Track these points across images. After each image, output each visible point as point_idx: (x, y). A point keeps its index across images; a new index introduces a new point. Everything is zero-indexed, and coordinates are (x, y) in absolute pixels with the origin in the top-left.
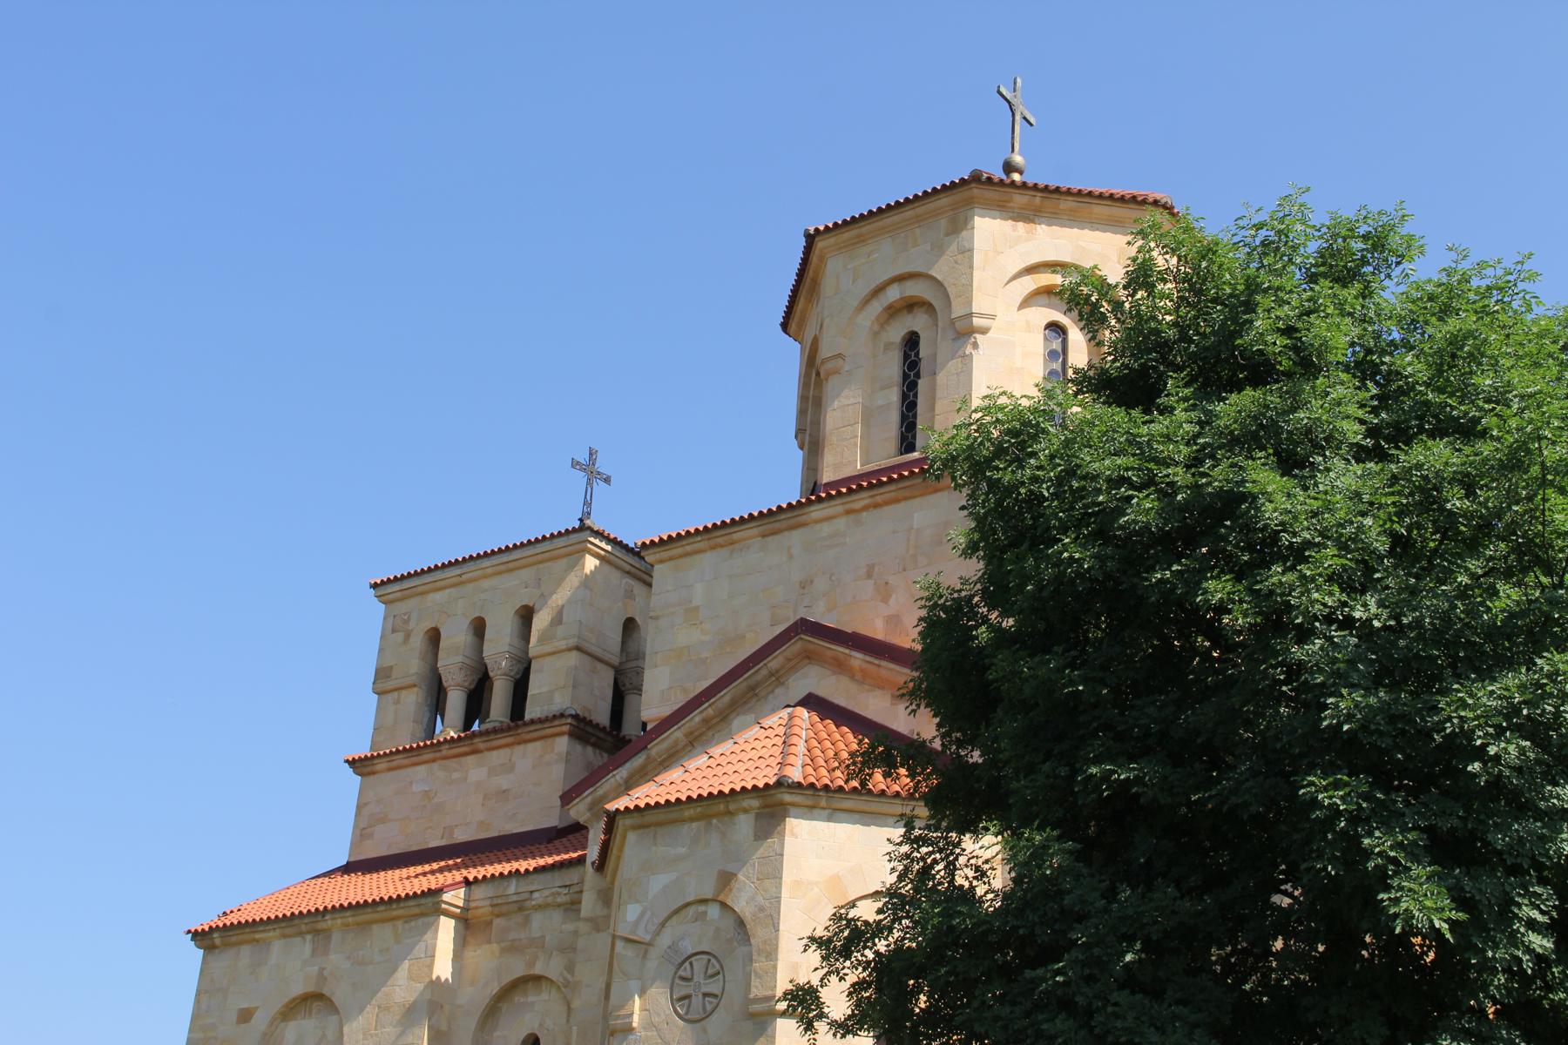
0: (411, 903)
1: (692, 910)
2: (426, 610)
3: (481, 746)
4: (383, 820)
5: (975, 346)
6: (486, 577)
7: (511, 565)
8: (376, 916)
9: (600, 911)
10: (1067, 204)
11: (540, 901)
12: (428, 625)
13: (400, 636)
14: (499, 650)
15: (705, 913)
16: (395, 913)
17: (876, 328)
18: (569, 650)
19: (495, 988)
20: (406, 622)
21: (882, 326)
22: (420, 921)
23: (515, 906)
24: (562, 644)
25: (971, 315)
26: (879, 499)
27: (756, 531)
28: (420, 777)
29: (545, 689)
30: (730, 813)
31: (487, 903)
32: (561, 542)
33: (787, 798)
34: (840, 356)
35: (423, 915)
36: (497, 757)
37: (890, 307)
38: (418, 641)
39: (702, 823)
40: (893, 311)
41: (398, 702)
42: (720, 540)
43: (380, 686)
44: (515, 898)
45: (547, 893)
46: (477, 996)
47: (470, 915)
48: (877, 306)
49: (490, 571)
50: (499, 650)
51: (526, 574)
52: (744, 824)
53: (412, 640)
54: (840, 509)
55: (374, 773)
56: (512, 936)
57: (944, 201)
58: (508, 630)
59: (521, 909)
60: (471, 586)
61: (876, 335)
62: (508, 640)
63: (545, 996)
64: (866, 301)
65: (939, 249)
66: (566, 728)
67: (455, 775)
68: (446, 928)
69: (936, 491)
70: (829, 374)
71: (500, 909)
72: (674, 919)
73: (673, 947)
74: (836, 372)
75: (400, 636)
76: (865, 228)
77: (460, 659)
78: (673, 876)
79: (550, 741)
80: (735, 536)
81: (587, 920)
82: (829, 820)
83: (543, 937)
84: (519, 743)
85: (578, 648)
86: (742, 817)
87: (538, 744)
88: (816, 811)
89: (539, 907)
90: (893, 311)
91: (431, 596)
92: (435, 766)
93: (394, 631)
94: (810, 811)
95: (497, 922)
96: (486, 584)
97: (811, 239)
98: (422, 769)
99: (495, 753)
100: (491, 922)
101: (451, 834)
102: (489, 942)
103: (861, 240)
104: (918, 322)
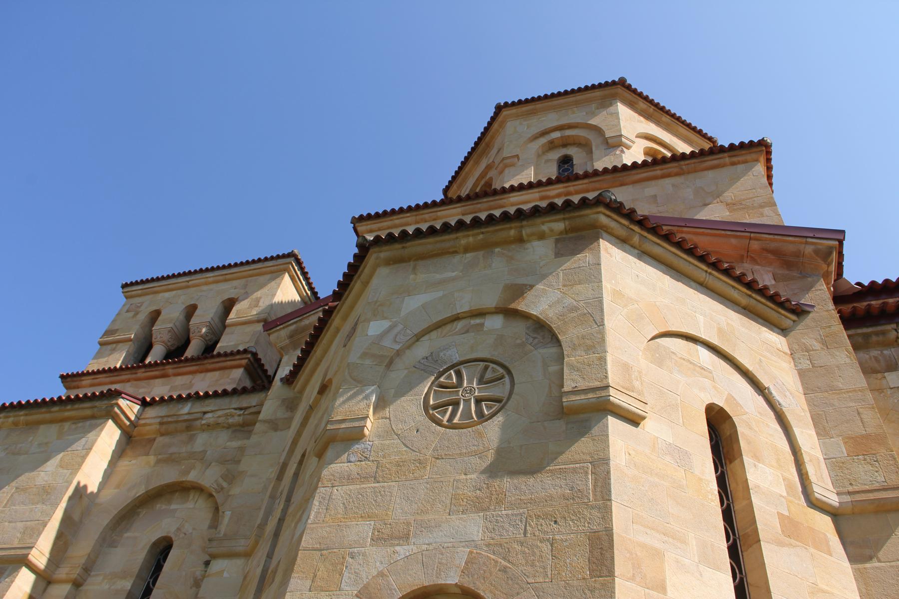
0: (87, 405)
1: (460, 325)
5: (622, 151)
6: (206, 284)
8: (48, 416)
9: (281, 414)
10: (666, 119)
11: (211, 421)
13: (131, 314)
15: (482, 325)
16: (67, 414)
17: (540, 152)
19: (141, 491)
20: (139, 307)
21: (544, 153)
22: (88, 423)
23: (184, 424)
25: (621, 136)
26: (572, 189)
27: (459, 210)
30: (520, 240)
31: (158, 420)
33: (603, 219)
34: (517, 156)
35: (93, 417)
37: (551, 142)
38: (143, 316)
39: (480, 254)
40: (552, 146)
42: (427, 216)
44: (186, 417)
45: (220, 413)
46: (117, 498)
47: (135, 432)
48: (543, 140)
50: (200, 326)
51: (235, 283)
52: (539, 250)
53: (138, 316)
54: (537, 195)
56: (173, 450)
57: (598, 93)
58: (214, 310)
59: (189, 428)
61: (539, 156)
62: (211, 315)
63: (190, 505)
64: (536, 137)
65: (593, 114)
66: (244, 362)
68: (108, 437)
69: (622, 185)
70: (506, 166)
71: (166, 428)
72: (434, 334)
73: (433, 358)
74: (513, 165)
75: (131, 314)
76: (539, 105)
77: (171, 325)
78: (440, 294)
79: (227, 371)
80: (439, 214)
81: (265, 421)
82: (639, 258)
83: (205, 452)
84: (201, 372)
86: (537, 244)
87: (217, 373)
88: (627, 247)
89: (209, 427)
90: (552, 146)
91: (161, 295)
93: (128, 311)
94: (623, 242)
95: (160, 440)
96: (205, 288)
97: (499, 108)
99: (179, 378)
100: (154, 439)
102: (147, 454)
103: (533, 113)
104: (571, 151)
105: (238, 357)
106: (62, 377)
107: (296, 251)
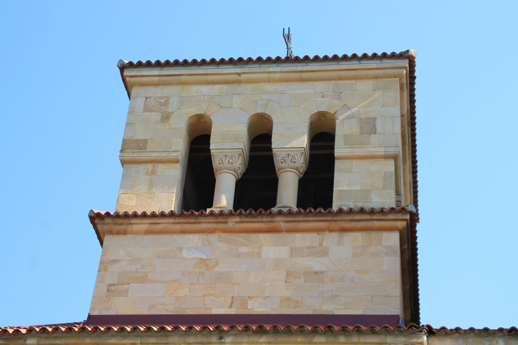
2: (197, 98)
3: (283, 225)
4: (142, 279)
6: (269, 81)
7: (304, 75)
12: (194, 111)
14: (291, 144)
18: (386, 157)
20: (166, 104)
24: (381, 151)
28: (194, 245)
29: (357, 188)
32: (373, 64)
36: (301, 240)
41: (153, 173)
43: (129, 155)
49: (278, 76)
51: (320, 86)
55: (125, 233)
60: (249, 86)
67: (243, 249)
75: (156, 116)
79: (374, 234)
85: (395, 158)
87: (358, 235)
91: (195, 89)
92: (214, 237)
96: (269, 87)
98: (195, 239)
101: (244, 304)
105: (391, 216)
106: (95, 218)
107: (412, 52)
